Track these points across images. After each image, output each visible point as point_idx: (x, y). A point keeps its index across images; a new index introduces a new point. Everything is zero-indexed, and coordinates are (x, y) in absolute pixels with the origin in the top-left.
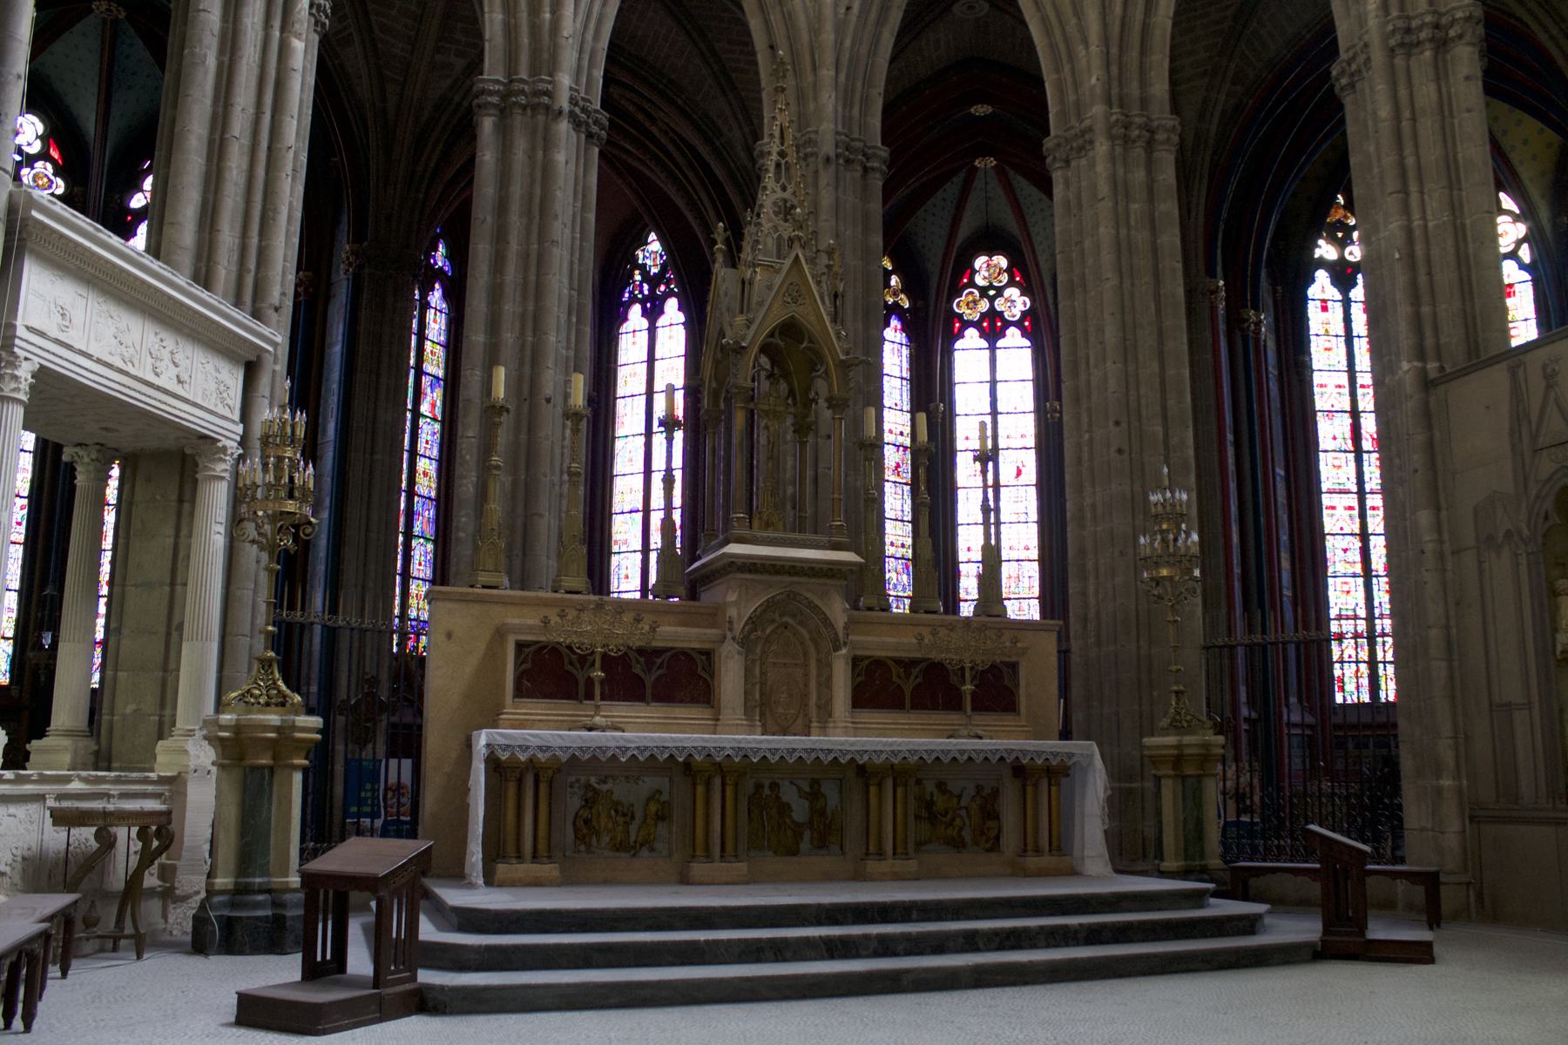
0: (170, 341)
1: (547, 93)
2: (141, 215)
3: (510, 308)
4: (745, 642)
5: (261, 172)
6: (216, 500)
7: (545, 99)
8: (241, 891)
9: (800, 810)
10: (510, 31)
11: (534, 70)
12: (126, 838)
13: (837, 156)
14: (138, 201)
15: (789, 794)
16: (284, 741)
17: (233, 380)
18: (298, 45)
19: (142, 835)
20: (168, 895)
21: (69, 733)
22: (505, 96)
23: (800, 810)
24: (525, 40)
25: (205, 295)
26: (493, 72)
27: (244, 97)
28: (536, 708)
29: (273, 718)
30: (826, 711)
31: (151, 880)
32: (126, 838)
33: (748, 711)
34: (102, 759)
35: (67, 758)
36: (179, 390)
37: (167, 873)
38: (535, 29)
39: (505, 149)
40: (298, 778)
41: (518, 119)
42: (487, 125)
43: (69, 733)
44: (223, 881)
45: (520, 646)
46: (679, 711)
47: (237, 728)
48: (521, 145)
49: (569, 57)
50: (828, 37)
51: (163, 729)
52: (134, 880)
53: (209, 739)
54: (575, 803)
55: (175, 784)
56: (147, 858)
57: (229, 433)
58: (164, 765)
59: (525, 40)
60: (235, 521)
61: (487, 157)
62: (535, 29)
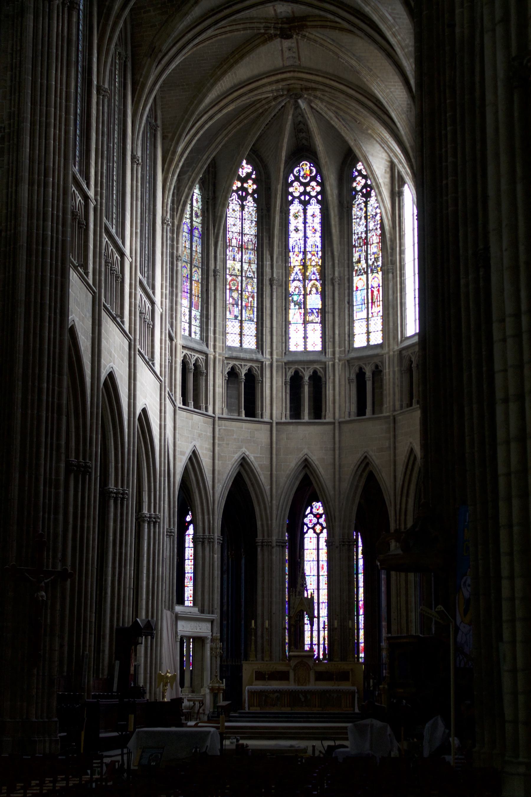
0: (198, 623)
1: (271, 542)
2: (190, 523)
3: (266, 593)
4: (294, 670)
5: (211, 583)
6: (208, 646)
7: (270, 543)
8: (214, 712)
9: (303, 700)
10: (262, 525)
11: (268, 536)
12: (197, 703)
13: (340, 545)
14: (189, 518)
15: (301, 696)
16: (219, 689)
17: (209, 625)
18: (216, 556)
19: (199, 703)
20: (204, 714)
21: (188, 687)
22: (262, 542)
23: (303, 700)
24: (265, 528)
25: (203, 615)
26: (259, 538)
27: (207, 568)
28: (258, 682)
29: (217, 685)
30: (309, 681)
31: (201, 711)
32: (197, 703)
33: (295, 682)
34: (193, 692)
35: (188, 692)
36: (200, 631)
37: (204, 710)
38: (267, 524)
39: (263, 555)
40: (221, 694)
41: (265, 548)
42: (259, 549)
43: (188, 687)
44: (212, 710)
45: (256, 672)
46: (283, 682)
47: (212, 687)
48: (266, 554)
49: (275, 531)
50: (337, 514)
51: (202, 687)
52: (199, 710)
53: (208, 688)
54: (264, 698)
55: (204, 695)
56: (200, 707)
57: (210, 637)
58: (202, 693)
59: (265, 528)
60: (211, 653)
61: (259, 557)
62: (267, 524)
